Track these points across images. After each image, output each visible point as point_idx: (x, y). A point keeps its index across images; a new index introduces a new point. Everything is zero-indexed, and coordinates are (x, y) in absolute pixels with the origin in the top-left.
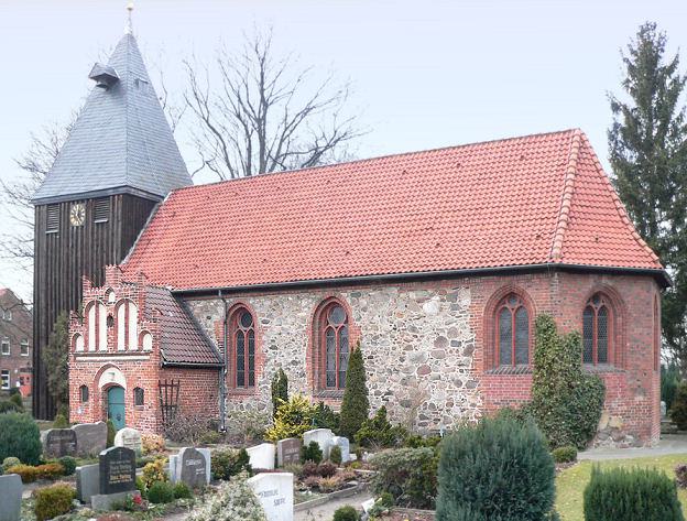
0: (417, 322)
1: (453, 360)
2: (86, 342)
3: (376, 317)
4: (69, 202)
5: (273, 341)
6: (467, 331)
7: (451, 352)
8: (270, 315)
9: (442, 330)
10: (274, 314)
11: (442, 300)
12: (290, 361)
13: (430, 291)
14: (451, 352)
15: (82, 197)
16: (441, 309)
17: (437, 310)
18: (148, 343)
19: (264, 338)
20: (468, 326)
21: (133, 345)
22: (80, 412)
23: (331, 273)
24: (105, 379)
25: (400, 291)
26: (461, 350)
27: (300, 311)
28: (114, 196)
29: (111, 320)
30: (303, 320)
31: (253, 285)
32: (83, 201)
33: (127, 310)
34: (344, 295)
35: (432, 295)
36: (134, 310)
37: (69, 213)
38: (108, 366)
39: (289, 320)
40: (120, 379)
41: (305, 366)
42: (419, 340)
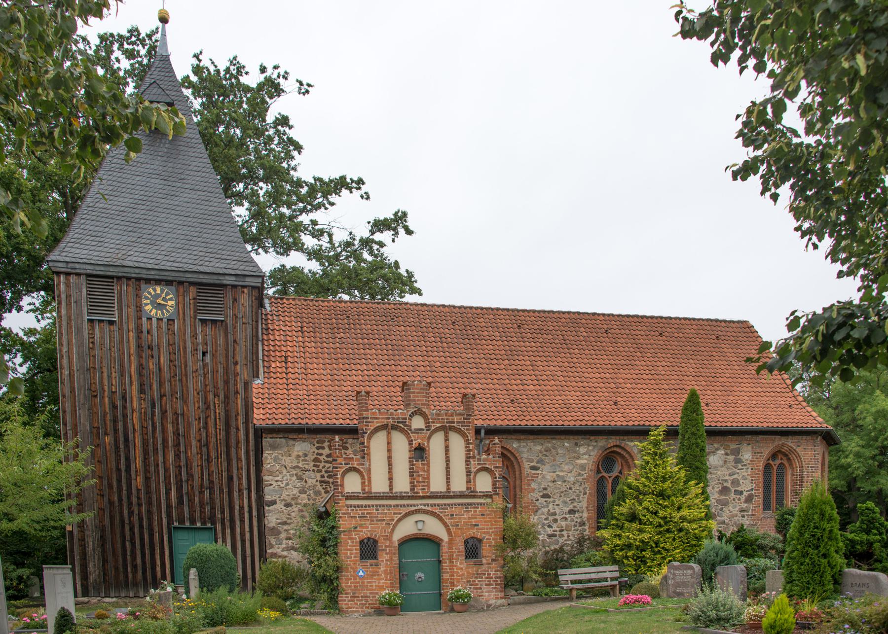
5: (545, 489)
6: (748, 482)
7: (734, 500)
8: (540, 461)
9: (726, 481)
13: (716, 445)
14: (734, 500)
15: (171, 276)
16: (725, 462)
17: (721, 463)
18: (484, 483)
19: (533, 485)
20: (749, 477)
21: (459, 484)
23: (618, 421)
24: (407, 528)
26: (743, 498)
27: (578, 458)
29: (420, 453)
30: (583, 467)
31: (578, 427)
35: (717, 449)
36: (457, 444)
39: (566, 468)
40: (433, 527)
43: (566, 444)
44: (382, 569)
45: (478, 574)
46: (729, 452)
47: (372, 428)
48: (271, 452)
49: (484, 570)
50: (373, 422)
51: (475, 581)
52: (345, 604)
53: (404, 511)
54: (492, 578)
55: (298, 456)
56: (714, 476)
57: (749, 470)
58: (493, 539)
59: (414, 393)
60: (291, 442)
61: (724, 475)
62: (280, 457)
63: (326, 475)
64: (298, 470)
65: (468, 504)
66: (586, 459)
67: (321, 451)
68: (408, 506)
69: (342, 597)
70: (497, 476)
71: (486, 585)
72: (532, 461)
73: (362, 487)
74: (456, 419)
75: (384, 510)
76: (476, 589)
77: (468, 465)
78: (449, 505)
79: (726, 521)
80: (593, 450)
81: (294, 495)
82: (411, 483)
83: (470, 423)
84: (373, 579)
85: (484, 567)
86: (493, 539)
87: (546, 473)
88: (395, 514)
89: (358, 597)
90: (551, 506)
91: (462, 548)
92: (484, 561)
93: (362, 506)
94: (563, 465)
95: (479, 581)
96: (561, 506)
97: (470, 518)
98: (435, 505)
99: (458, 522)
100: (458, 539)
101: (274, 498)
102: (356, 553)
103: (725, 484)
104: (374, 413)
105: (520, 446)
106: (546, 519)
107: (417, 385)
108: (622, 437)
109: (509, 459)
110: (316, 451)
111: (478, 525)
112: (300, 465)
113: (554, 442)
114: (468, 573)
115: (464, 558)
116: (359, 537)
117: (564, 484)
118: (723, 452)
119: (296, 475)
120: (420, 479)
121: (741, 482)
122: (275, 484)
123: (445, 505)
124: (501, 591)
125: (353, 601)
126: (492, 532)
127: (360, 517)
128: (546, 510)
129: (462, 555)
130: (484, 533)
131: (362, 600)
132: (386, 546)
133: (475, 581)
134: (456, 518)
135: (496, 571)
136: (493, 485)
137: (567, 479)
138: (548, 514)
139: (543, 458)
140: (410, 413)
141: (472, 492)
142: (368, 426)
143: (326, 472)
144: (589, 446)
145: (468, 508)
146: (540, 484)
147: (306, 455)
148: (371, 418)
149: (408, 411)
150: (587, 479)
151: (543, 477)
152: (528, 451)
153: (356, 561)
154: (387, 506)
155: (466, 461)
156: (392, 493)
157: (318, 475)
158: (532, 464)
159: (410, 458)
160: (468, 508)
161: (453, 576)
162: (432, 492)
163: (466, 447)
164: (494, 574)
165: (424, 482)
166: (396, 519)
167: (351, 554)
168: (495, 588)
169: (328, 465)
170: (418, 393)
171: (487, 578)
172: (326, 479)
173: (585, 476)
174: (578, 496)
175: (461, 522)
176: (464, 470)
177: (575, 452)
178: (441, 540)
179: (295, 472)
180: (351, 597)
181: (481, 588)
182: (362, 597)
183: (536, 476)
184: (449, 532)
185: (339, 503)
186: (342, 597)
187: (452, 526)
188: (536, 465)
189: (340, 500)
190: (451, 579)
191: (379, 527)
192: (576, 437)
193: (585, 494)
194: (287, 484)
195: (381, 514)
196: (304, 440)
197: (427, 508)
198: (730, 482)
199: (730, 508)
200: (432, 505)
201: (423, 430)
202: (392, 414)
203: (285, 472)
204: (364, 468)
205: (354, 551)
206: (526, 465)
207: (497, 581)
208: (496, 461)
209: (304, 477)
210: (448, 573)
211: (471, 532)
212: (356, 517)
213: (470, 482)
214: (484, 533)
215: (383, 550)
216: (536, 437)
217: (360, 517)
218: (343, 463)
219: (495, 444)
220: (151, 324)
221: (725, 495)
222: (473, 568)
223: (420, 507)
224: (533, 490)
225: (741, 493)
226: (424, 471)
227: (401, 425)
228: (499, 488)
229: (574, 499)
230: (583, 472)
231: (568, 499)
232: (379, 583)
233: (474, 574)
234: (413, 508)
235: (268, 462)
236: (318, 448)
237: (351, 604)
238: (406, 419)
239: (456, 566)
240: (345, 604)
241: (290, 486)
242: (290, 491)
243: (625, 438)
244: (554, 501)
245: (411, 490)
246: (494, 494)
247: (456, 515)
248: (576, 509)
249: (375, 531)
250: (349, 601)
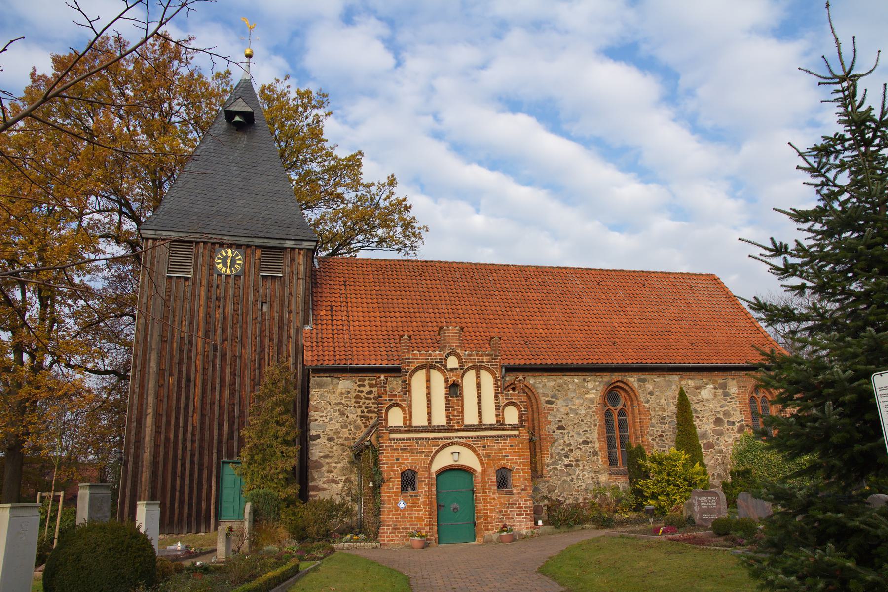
0: (698, 405)
1: (729, 437)
2: (408, 414)
3: (663, 401)
4: (213, 244)
5: (560, 421)
6: (738, 413)
7: (728, 430)
10: (559, 395)
11: (715, 388)
12: (581, 440)
14: (728, 430)
16: (715, 395)
17: (712, 396)
18: (512, 416)
19: (550, 418)
20: (738, 409)
21: (490, 418)
22: (402, 505)
23: (618, 359)
24: (444, 460)
25: (681, 378)
26: (736, 428)
27: (587, 393)
28: (293, 249)
29: (454, 389)
30: (592, 401)
32: (239, 246)
33: (478, 377)
34: (632, 380)
35: (707, 384)
36: (487, 380)
37: (212, 258)
38: (452, 444)
39: (577, 401)
40: (468, 459)
41: (597, 445)
42: (700, 421)
43: (576, 381)
44: (421, 500)
45: (509, 504)
46: (717, 386)
47: (413, 368)
48: (318, 390)
49: (515, 500)
50: (414, 362)
51: (506, 511)
52: (387, 537)
53: (441, 443)
54: (522, 507)
55: (342, 394)
56: (707, 408)
57: (737, 402)
58: (522, 469)
59: (449, 336)
60: (336, 381)
61: (716, 407)
62: (326, 394)
63: (365, 411)
64: (341, 406)
65: (499, 436)
66: (594, 393)
67: (361, 389)
68: (445, 438)
69: (384, 529)
70: (523, 409)
71: (517, 515)
72: (547, 396)
73: (404, 421)
74: (485, 359)
75: (423, 443)
76: (508, 519)
77: (496, 400)
78: (481, 437)
79: (724, 451)
80: (599, 386)
81: (337, 429)
82: (447, 417)
83: (497, 362)
84: (412, 510)
85: (515, 497)
86: (522, 469)
87: (560, 405)
88: (433, 446)
89: (399, 529)
90: (566, 437)
91: (494, 479)
92: (515, 491)
93: (403, 439)
94: (574, 399)
95: (511, 511)
96: (575, 437)
97: (500, 449)
98: (469, 437)
99: (490, 453)
100: (490, 469)
101: (318, 433)
102: (398, 485)
103: (718, 416)
104: (415, 355)
105: (535, 383)
106: (563, 450)
107: (452, 329)
108: (623, 374)
109: (531, 395)
110: (358, 389)
111: (507, 456)
112: (343, 401)
113: (565, 378)
114: (501, 503)
115: (496, 488)
116: (401, 469)
117: (576, 417)
118: (712, 386)
119: (339, 410)
120: (456, 413)
121: (732, 413)
122: (319, 419)
123: (478, 437)
124: (531, 521)
125: (394, 533)
126: (521, 463)
127: (401, 450)
128: (562, 441)
129: (494, 485)
130: (514, 463)
131: (402, 532)
132: (425, 478)
133: (506, 511)
134: (488, 450)
135: (525, 501)
136: (519, 418)
137: (579, 412)
138: (565, 445)
139: (557, 392)
140: (446, 354)
141: (501, 425)
142: (409, 366)
143: (366, 407)
144: (595, 381)
145: (498, 440)
146: (555, 417)
147: (348, 393)
148: (413, 359)
149: (444, 353)
150: (596, 412)
151: (558, 411)
152: (543, 387)
153: (398, 492)
154: (426, 439)
155: (495, 397)
156: (430, 426)
157: (359, 410)
158: (547, 399)
160: (498, 440)
161: (487, 506)
162: (466, 426)
163: (495, 384)
164: (524, 504)
165: (459, 416)
166: (434, 452)
167: (393, 486)
168: (525, 518)
169: (367, 401)
170: (453, 336)
171: (518, 508)
172: (365, 414)
173: (594, 409)
174: (589, 427)
175: (492, 453)
176: (493, 406)
177: (584, 387)
178: (474, 470)
179: (338, 408)
180: (393, 529)
181: (512, 518)
182: (402, 528)
183: (551, 409)
184: (482, 463)
185: (382, 436)
186: (384, 529)
187: (485, 457)
188: (550, 399)
189: (384, 433)
190: (485, 509)
191: (418, 459)
192: (584, 374)
193: (595, 425)
194: (331, 420)
195: (421, 446)
196: (347, 379)
197: (461, 440)
198: (722, 413)
199: (726, 438)
200: (466, 438)
201: (457, 368)
202: (430, 355)
203: (329, 408)
204: (405, 404)
205: (396, 483)
206: (543, 399)
207: (527, 511)
208: (522, 396)
209: (346, 412)
210: (481, 503)
211: (502, 462)
212: (397, 450)
213: (499, 415)
214: (514, 463)
215: (422, 481)
216: (549, 374)
217: (401, 450)
218: (388, 399)
219: (520, 381)
221: (719, 426)
222: (505, 497)
223: (456, 440)
224: (550, 422)
225: (733, 423)
226: (459, 406)
227: (438, 364)
228: (524, 421)
229: (586, 431)
230: (592, 406)
231: (581, 431)
232: (418, 514)
233: (506, 504)
234: (449, 441)
235: (315, 399)
236: (359, 386)
237: (392, 537)
238: (442, 359)
239: (489, 496)
240: (387, 537)
241: (333, 421)
242: (333, 425)
243: (626, 374)
244: (569, 433)
245: (447, 423)
246: (521, 427)
247: (488, 446)
248: (588, 440)
249: (415, 463)
250: (391, 533)
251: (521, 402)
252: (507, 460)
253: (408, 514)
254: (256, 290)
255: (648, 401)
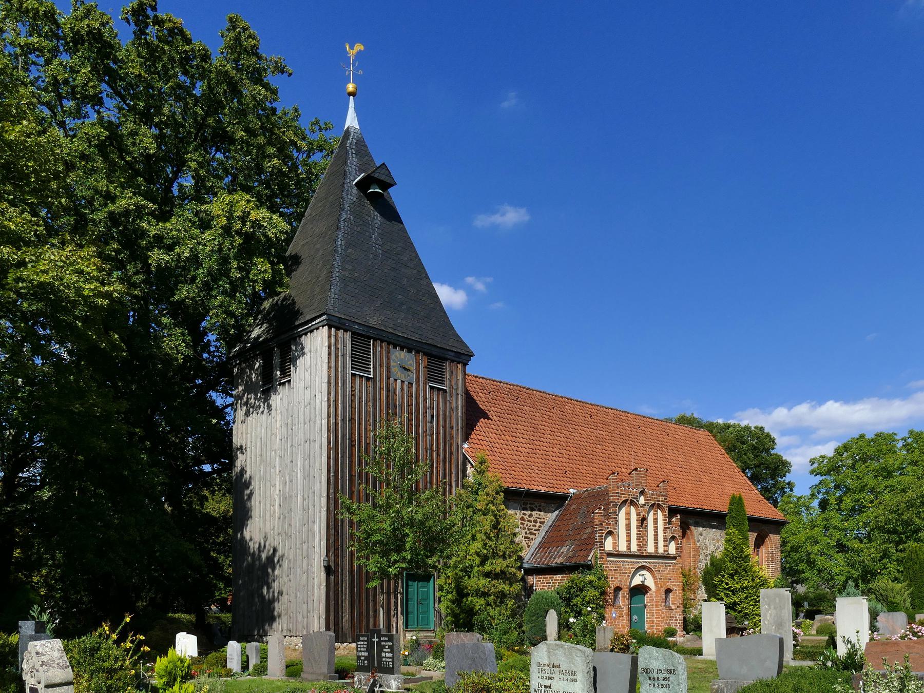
50: (621, 497)
53: (636, 566)
63: (528, 532)
111: (670, 579)
130: (675, 585)
136: (676, 549)
143: (529, 529)
156: (630, 552)
157: (523, 531)
159: (637, 526)
169: (529, 524)
171: (675, 620)
172: (528, 535)
184: (656, 583)
220: (396, 385)
227: (635, 500)
245: (638, 550)
251: (679, 536)
252: (671, 582)
253: (618, 622)
254: (425, 400)
255: (699, 541)
